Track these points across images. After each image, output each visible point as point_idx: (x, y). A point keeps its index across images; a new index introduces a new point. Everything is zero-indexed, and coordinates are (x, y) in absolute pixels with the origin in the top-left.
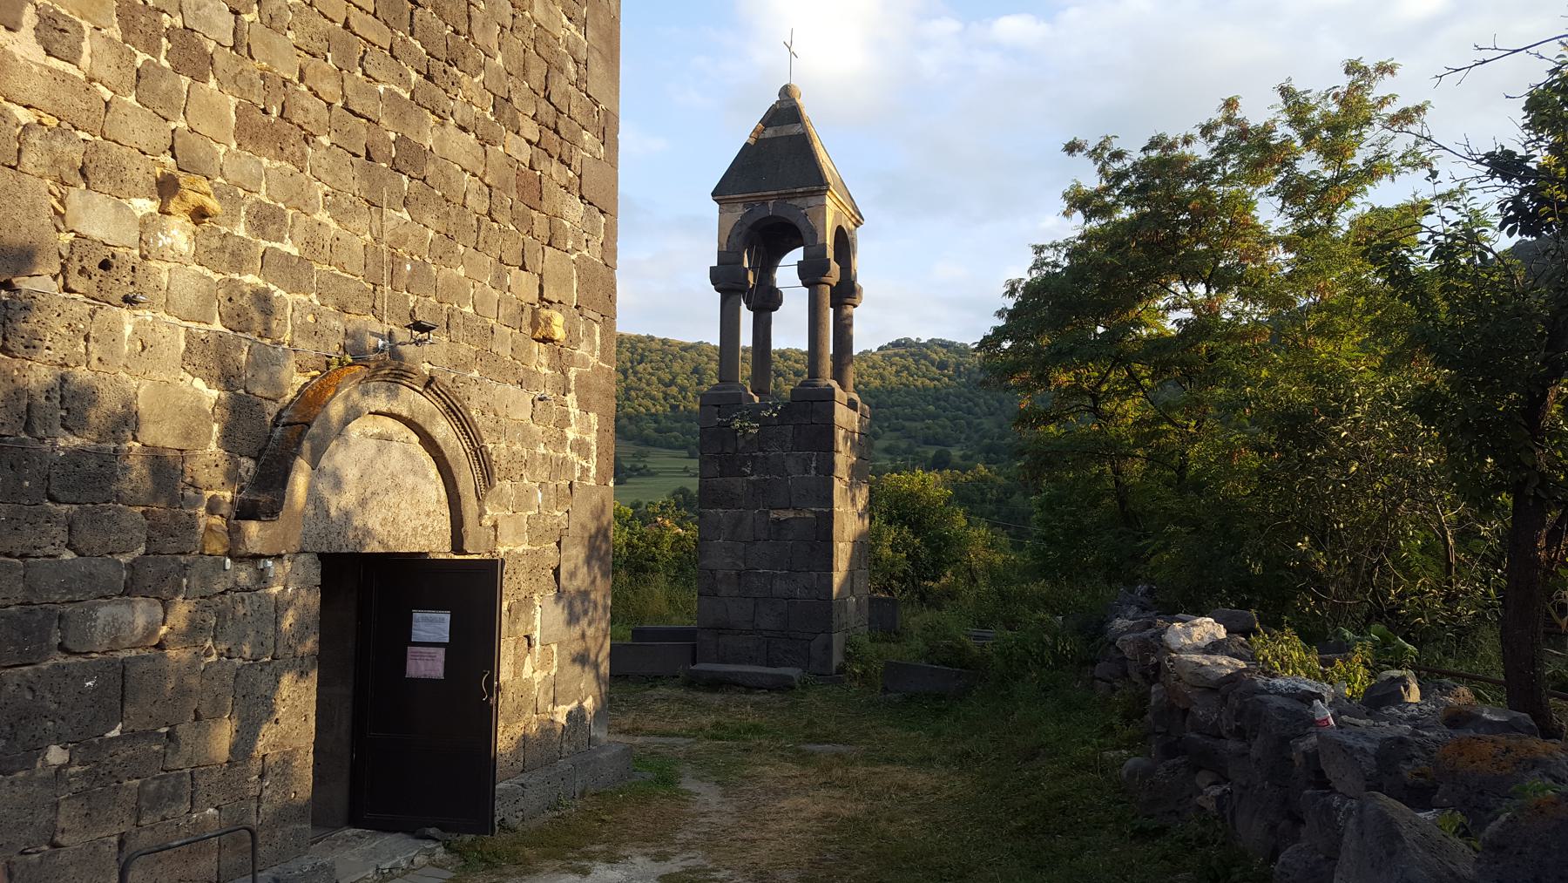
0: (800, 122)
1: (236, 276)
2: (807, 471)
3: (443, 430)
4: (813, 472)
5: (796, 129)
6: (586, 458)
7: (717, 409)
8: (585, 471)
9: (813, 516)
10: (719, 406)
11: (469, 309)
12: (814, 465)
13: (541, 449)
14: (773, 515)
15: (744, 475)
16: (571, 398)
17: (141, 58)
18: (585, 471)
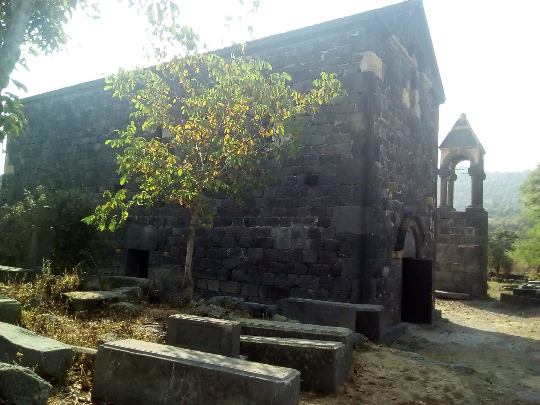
0: (467, 125)
1: (395, 201)
2: (471, 233)
3: (417, 229)
4: (473, 234)
5: (465, 127)
6: (432, 233)
7: (440, 213)
8: (433, 236)
9: (473, 247)
10: (440, 212)
11: (418, 200)
12: (473, 231)
13: (427, 232)
14: (460, 246)
15: (449, 233)
16: (431, 218)
17: (389, 161)
18: (433, 236)
